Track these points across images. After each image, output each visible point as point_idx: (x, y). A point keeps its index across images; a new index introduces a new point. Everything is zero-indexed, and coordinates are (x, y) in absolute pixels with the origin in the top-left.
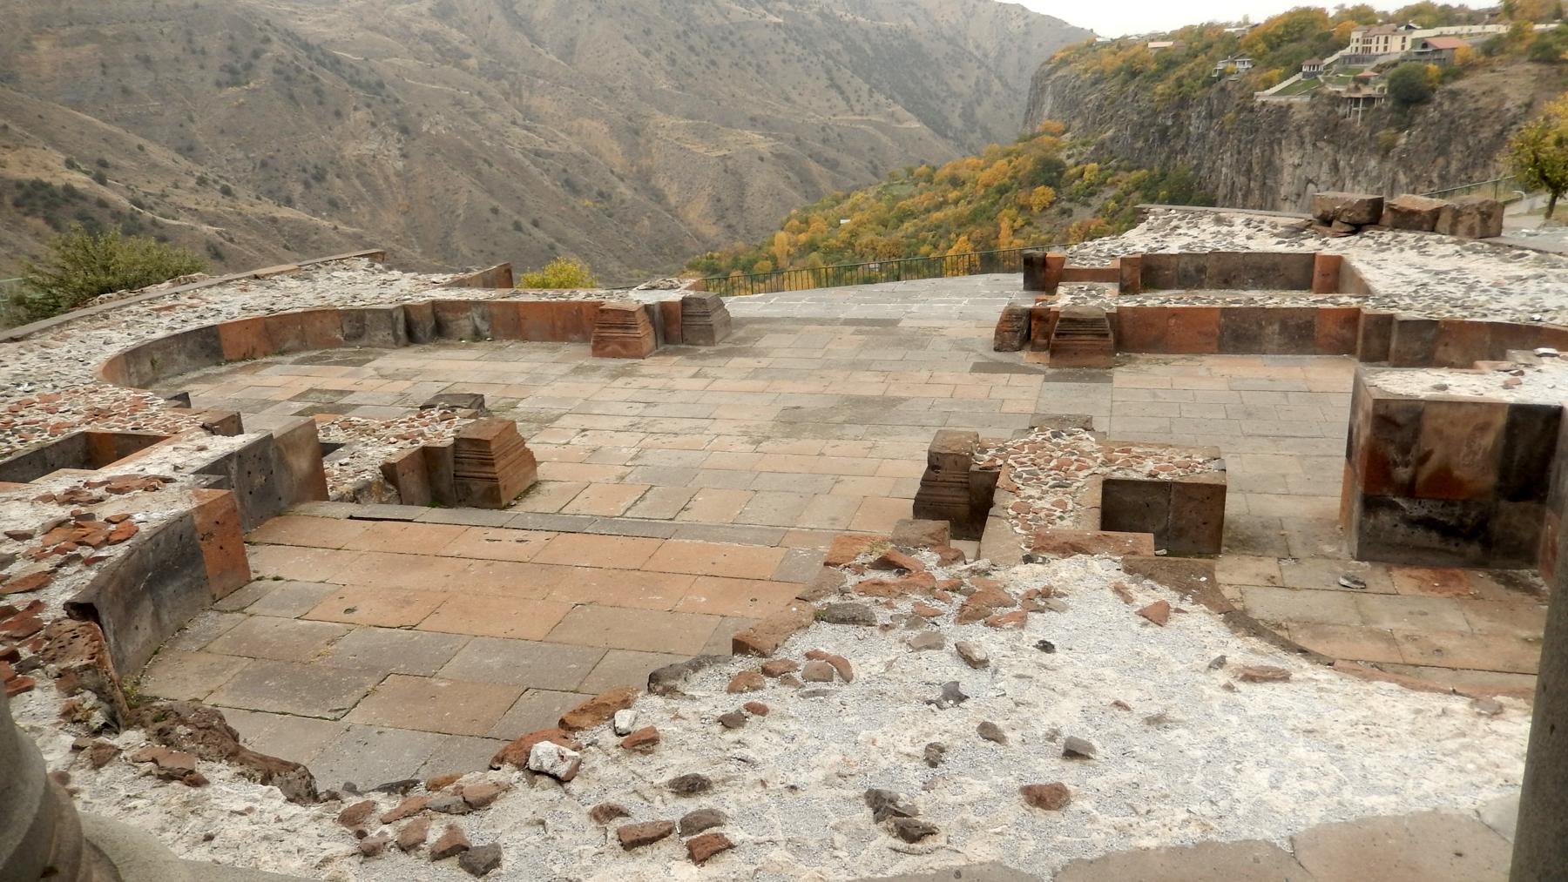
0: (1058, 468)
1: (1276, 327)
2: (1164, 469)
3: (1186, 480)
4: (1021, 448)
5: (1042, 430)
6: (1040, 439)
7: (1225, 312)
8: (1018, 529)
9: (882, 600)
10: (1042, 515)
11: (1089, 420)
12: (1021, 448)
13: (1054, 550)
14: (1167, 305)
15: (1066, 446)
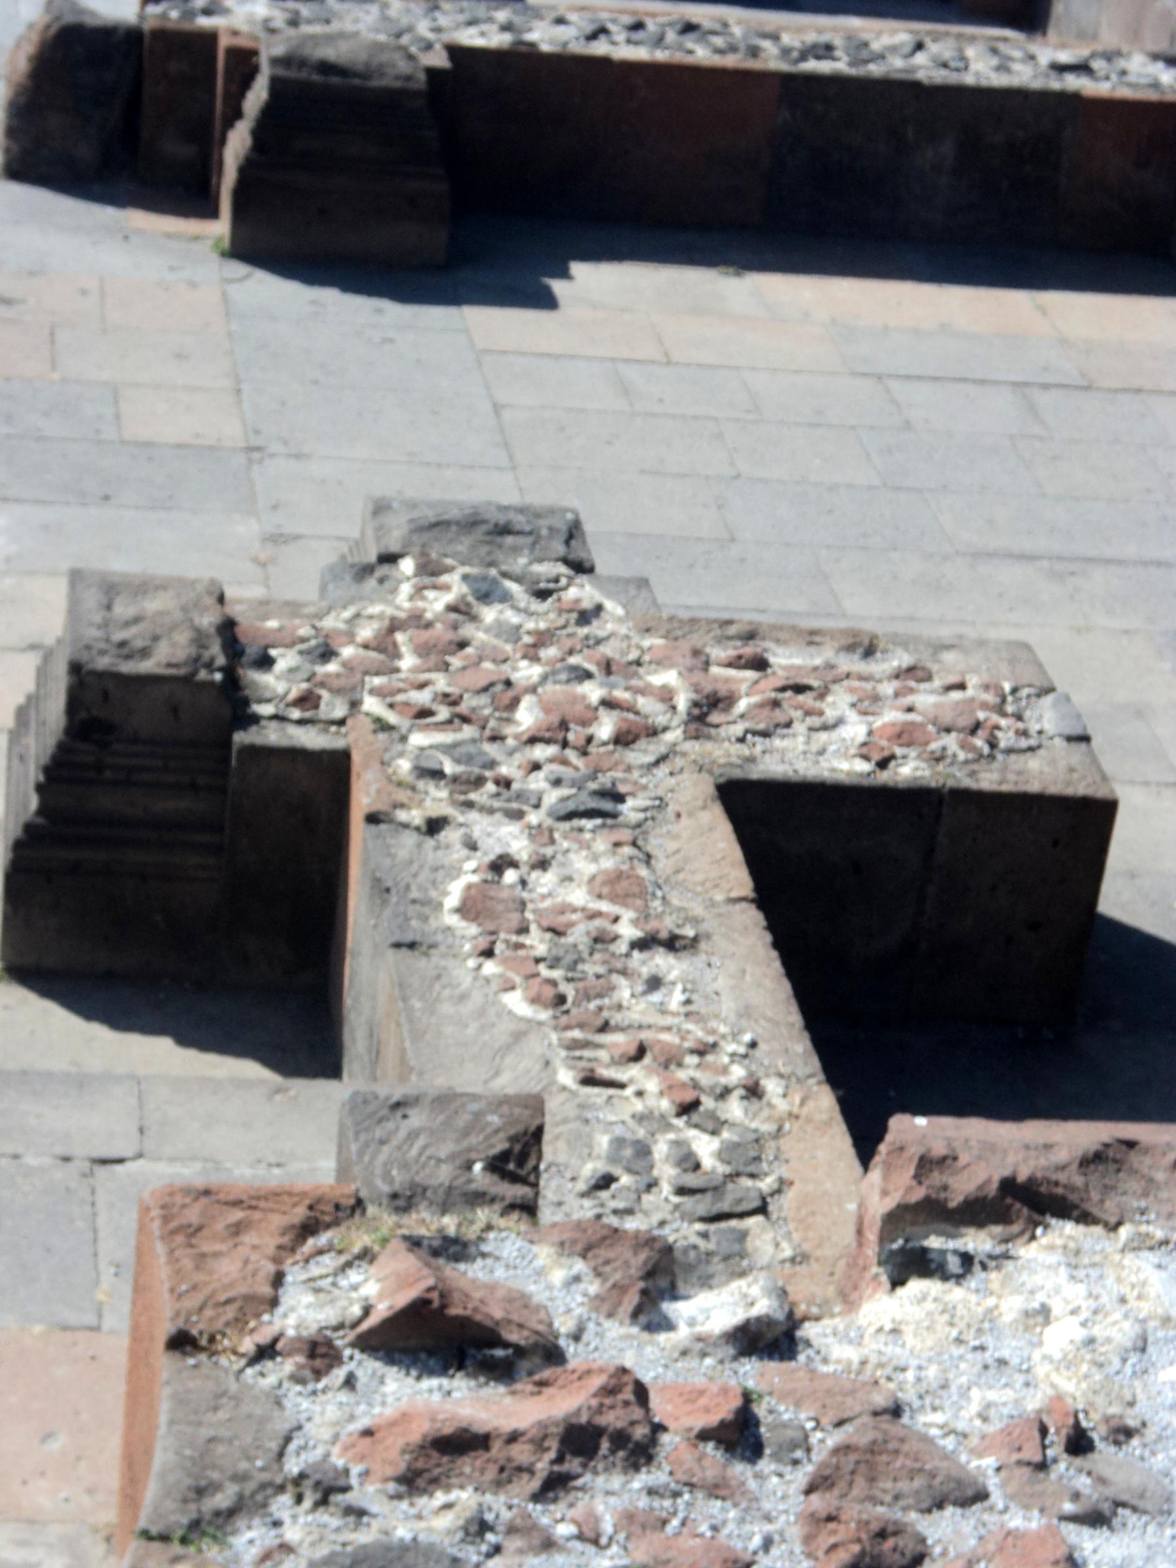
0: (556, 732)
1: (947, 149)
2: (905, 735)
3: (988, 780)
4: (385, 645)
5: (430, 570)
6: (436, 603)
7: (797, 89)
8: (516, 1002)
9: (499, 1506)
10: (579, 935)
11: (574, 532)
12: (385, 645)
13: (977, 1212)
14: (600, 48)
15: (542, 639)
